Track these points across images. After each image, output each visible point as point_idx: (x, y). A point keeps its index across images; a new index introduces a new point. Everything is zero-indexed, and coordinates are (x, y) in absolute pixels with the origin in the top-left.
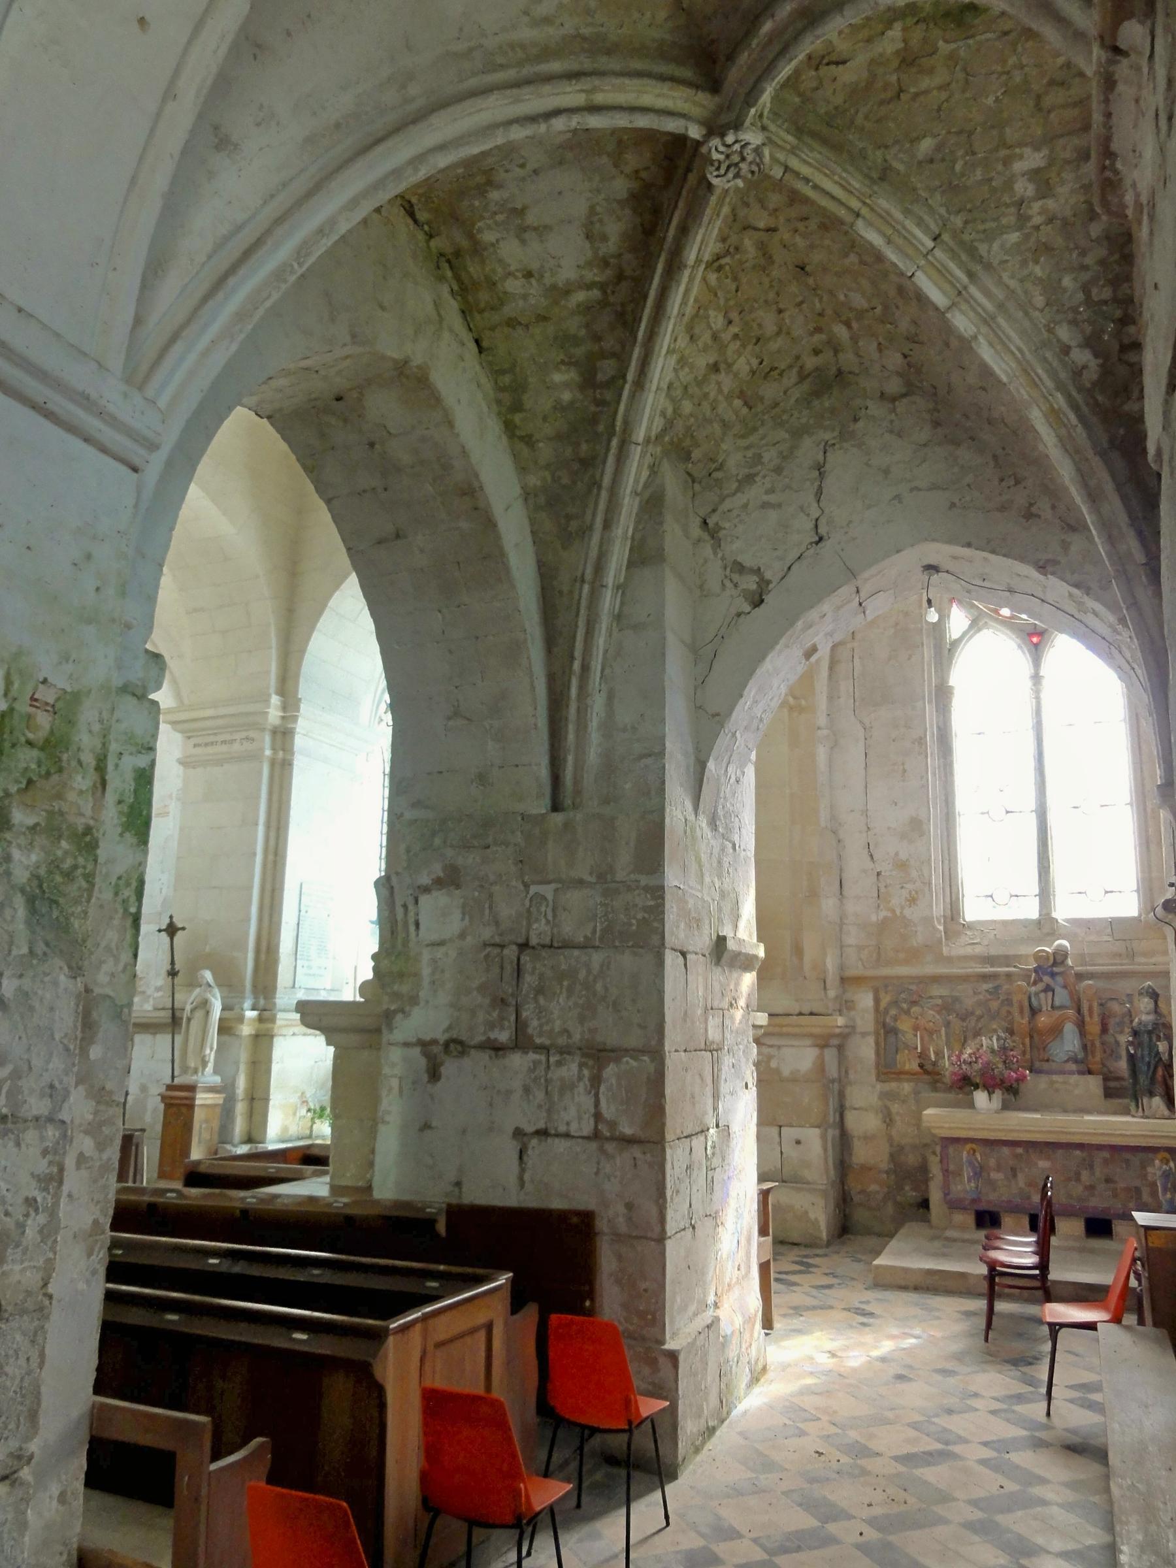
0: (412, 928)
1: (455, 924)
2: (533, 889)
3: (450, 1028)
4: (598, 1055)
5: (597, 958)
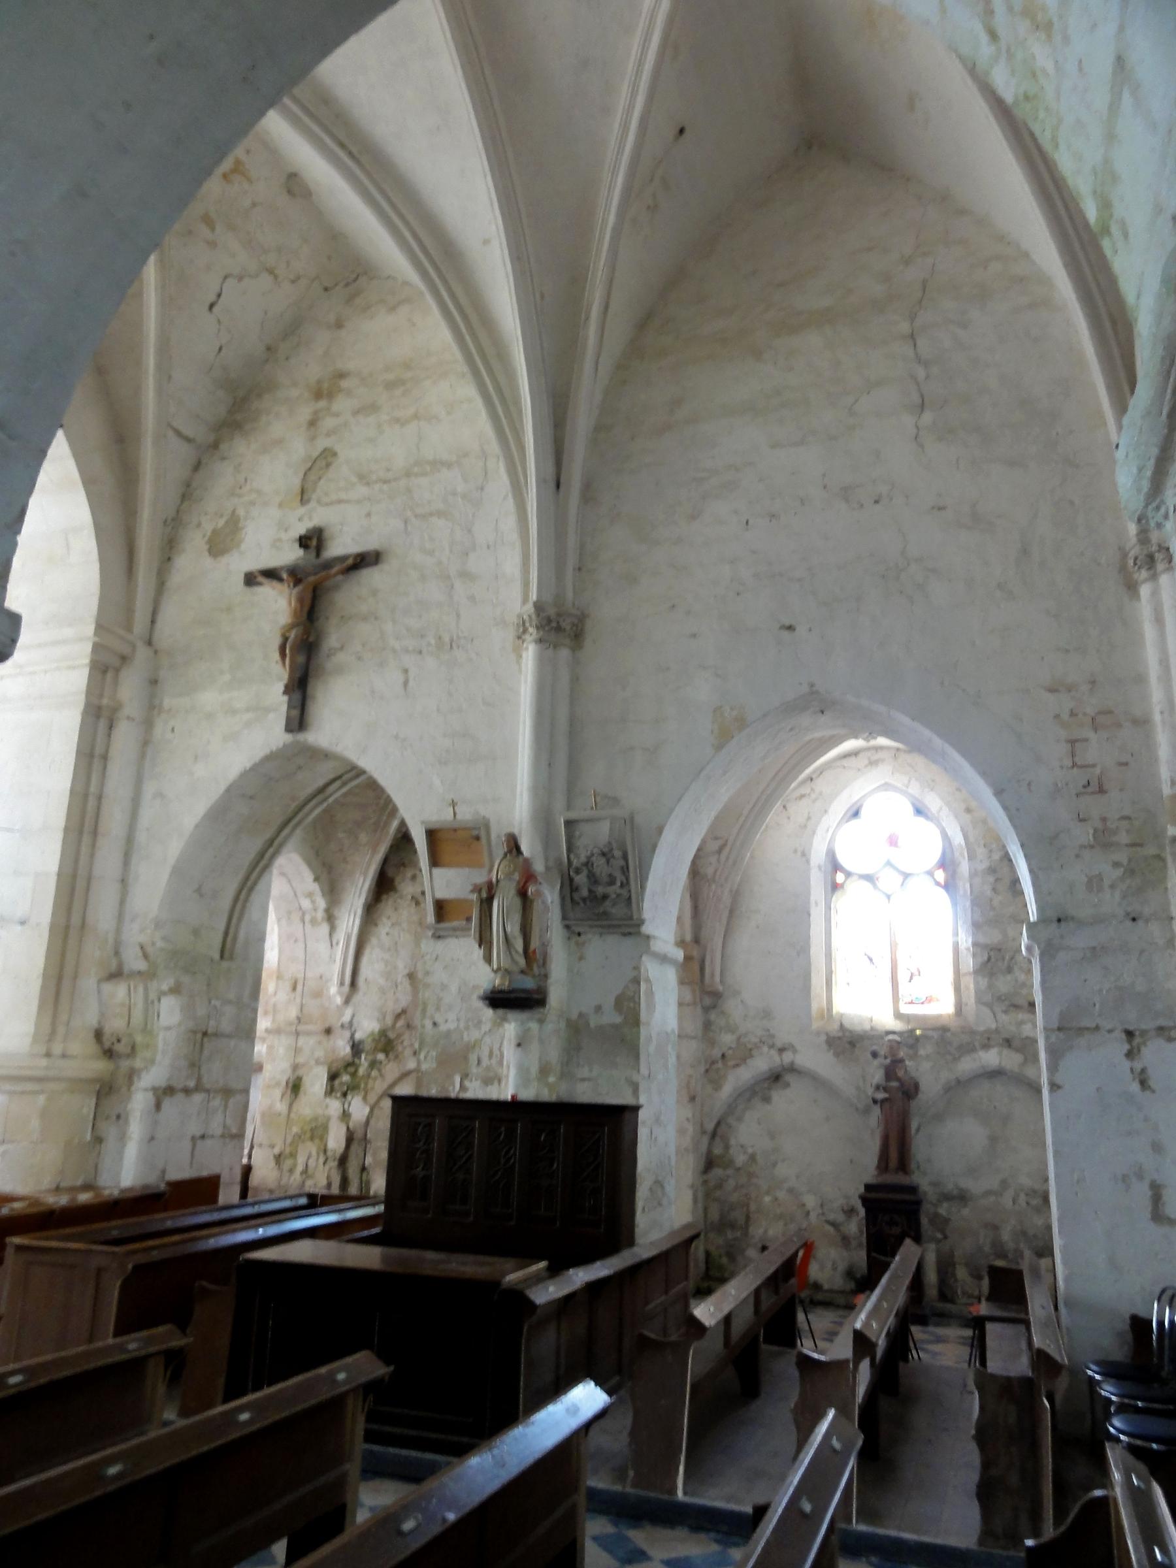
3: (169, 1080)
4: (227, 1092)
5: (232, 1043)
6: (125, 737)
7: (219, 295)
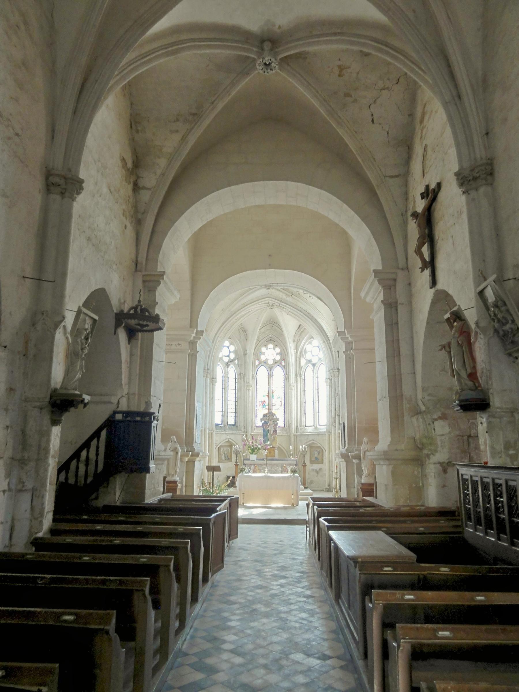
0: (433, 431)
1: (447, 430)
2: (471, 421)
3: (448, 459)
6: (402, 311)
7: (372, 115)
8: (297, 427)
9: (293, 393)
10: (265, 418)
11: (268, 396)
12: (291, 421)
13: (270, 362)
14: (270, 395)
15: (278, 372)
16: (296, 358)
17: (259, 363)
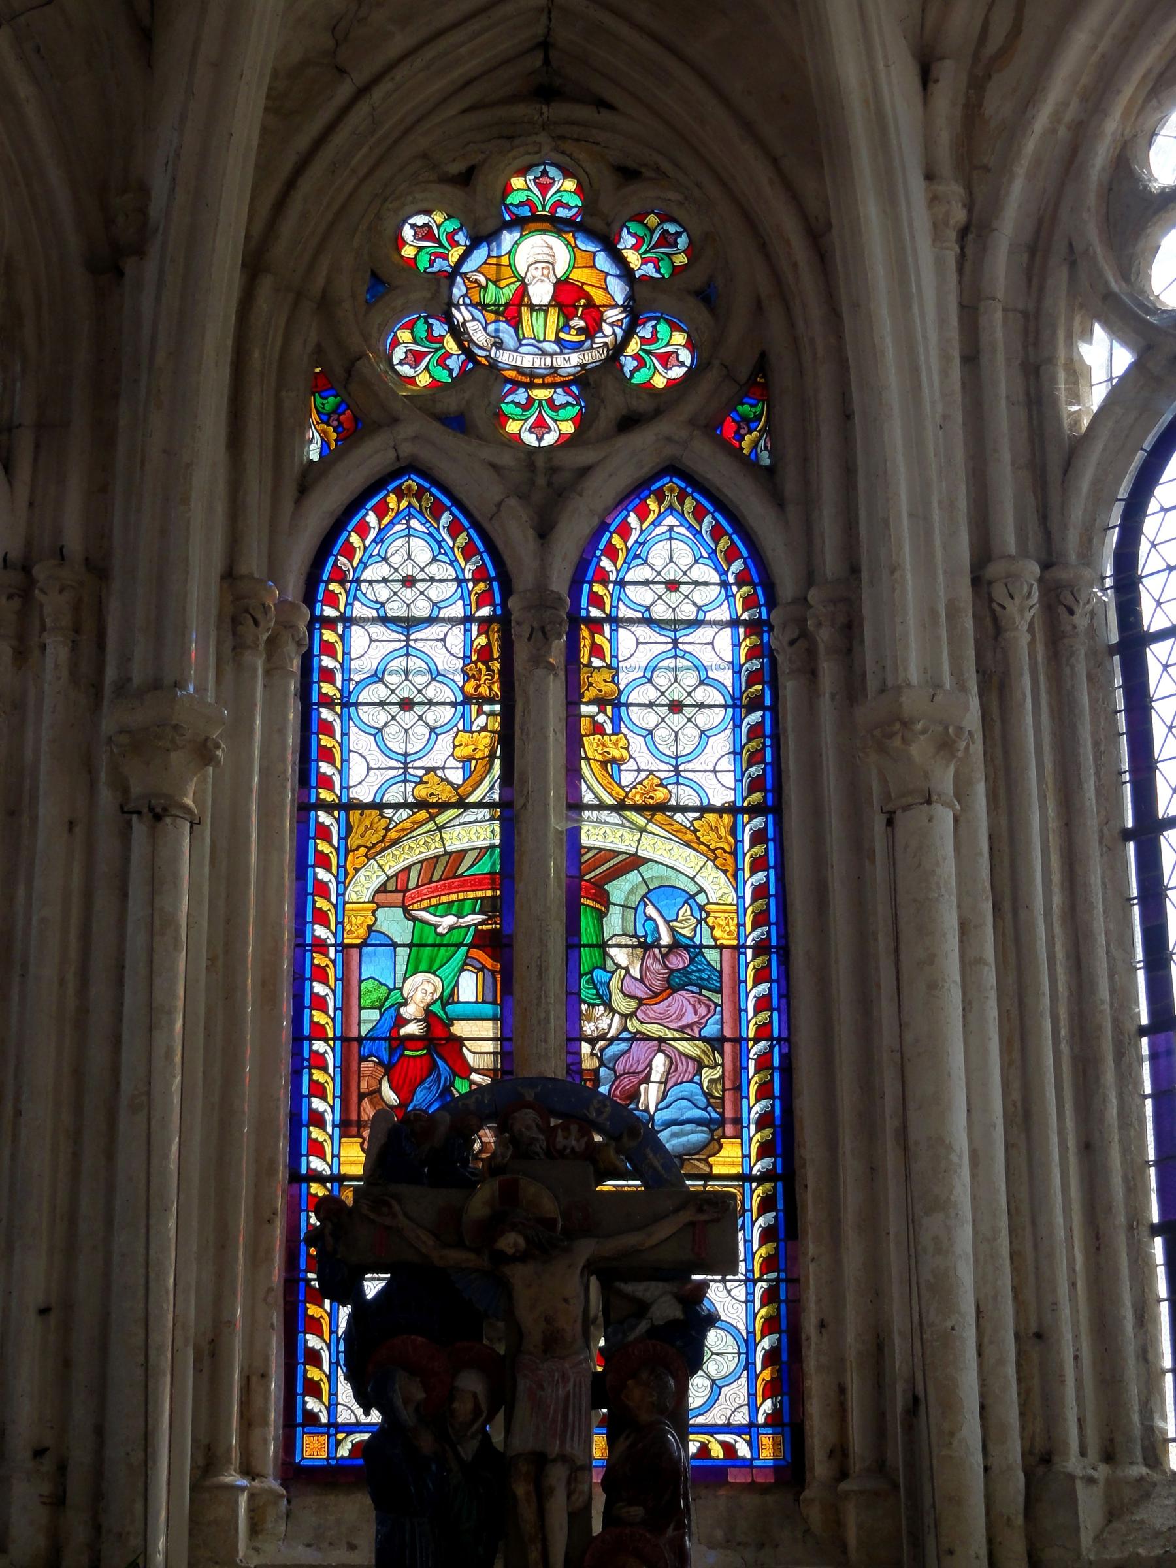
8: (1041, 1460)
9: (948, 846)
10: (420, 1204)
11: (496, 946)
12: (931, 1345)
13: (542, 425)
14: (533, 907)
15: (674, 619)
16: (970, 313)
17: (353, 430)
